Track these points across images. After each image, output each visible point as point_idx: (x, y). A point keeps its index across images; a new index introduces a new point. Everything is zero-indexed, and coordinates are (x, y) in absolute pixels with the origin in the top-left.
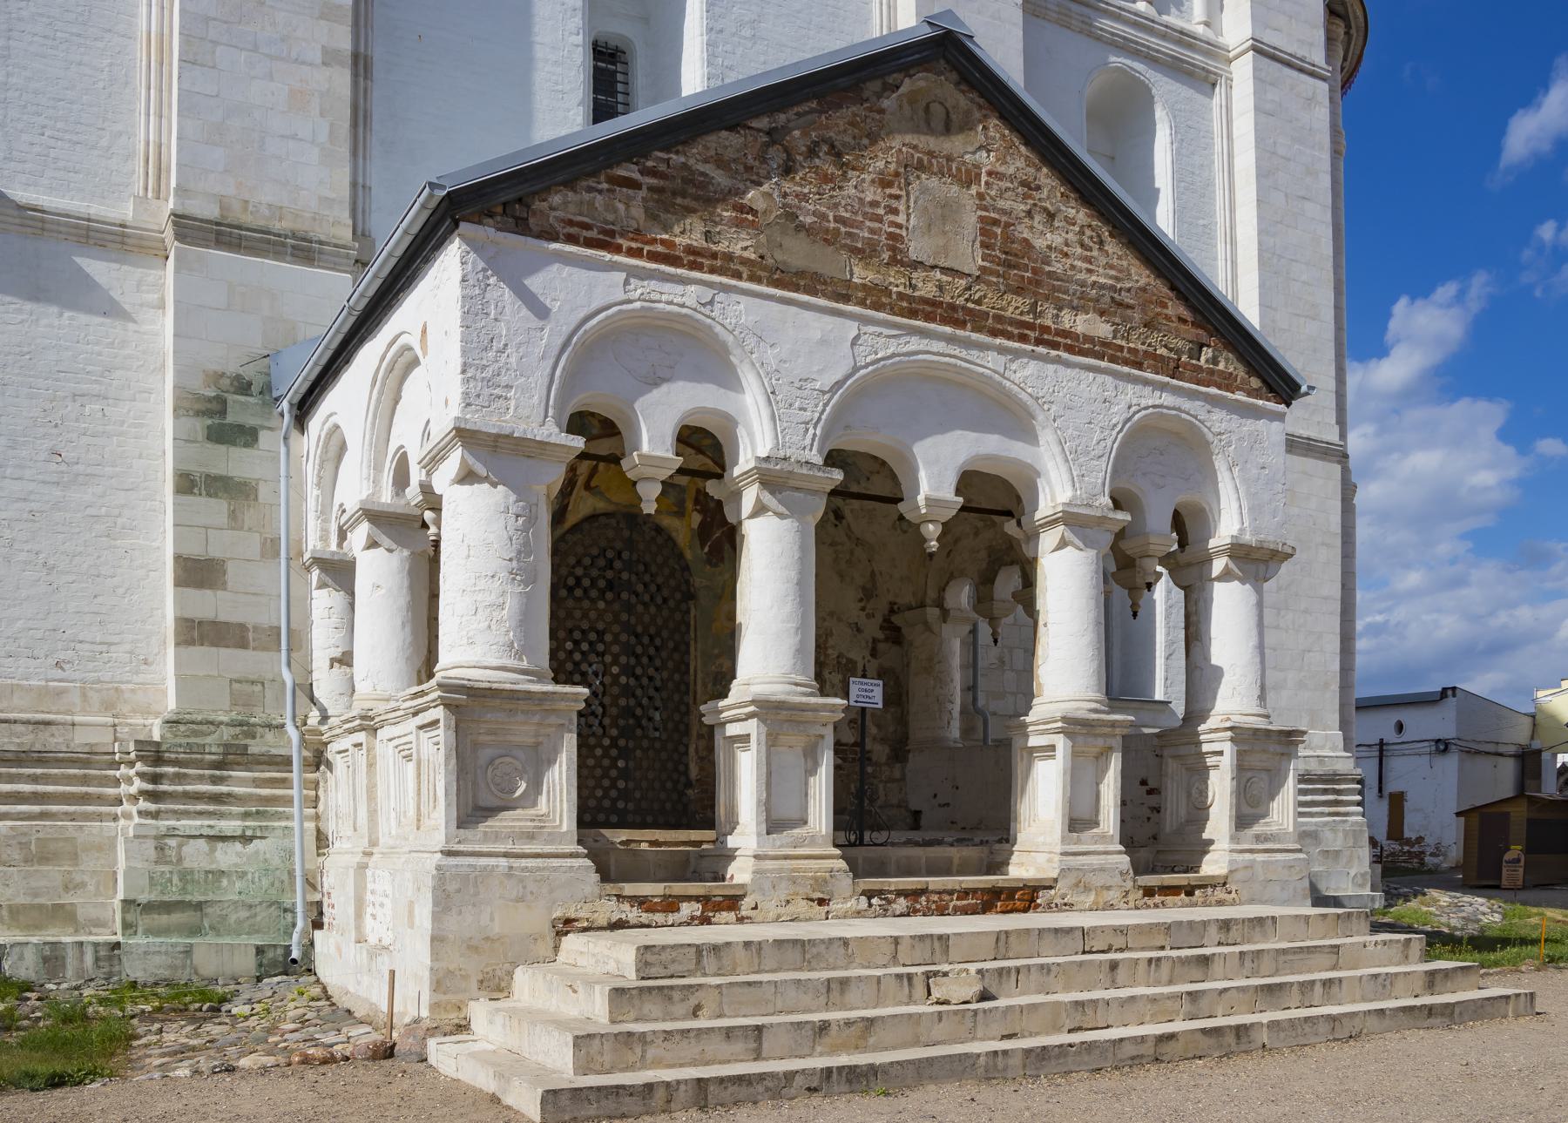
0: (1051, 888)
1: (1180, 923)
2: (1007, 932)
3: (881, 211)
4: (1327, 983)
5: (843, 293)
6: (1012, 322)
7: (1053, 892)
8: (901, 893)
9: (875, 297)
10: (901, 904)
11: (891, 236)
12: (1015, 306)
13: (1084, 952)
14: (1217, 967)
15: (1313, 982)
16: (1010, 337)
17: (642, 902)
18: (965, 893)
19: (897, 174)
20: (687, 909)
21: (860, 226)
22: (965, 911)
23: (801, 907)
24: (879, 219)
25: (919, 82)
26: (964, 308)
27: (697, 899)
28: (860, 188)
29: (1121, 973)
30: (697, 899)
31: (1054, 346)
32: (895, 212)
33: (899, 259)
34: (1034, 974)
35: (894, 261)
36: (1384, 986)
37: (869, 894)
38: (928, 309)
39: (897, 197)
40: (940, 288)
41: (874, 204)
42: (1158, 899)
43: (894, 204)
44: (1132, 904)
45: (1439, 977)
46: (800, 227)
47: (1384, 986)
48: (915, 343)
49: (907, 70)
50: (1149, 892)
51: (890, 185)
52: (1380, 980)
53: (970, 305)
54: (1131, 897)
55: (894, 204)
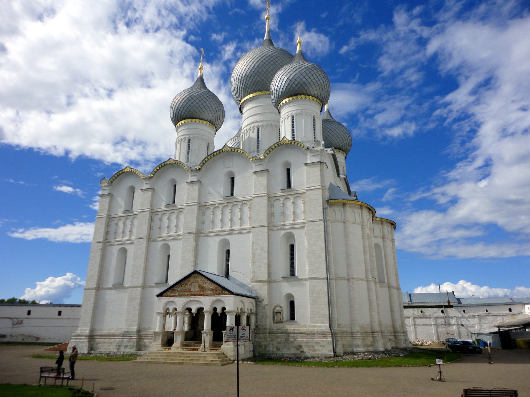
4: (198, 360)
5: (185, 296)
9: (187, 295)
10: (185, 349)
12: (202, 293)
17: (164, 349)
18: (191, 349)
20: (167, 349)
23: (176, 349)
25: (194, 275)
28: (188, 286)
33: (190, 291)
37: (182, 348)
46: (182, 291)
48: (191, 298)
49: (192, 274)
50: (211, 350)
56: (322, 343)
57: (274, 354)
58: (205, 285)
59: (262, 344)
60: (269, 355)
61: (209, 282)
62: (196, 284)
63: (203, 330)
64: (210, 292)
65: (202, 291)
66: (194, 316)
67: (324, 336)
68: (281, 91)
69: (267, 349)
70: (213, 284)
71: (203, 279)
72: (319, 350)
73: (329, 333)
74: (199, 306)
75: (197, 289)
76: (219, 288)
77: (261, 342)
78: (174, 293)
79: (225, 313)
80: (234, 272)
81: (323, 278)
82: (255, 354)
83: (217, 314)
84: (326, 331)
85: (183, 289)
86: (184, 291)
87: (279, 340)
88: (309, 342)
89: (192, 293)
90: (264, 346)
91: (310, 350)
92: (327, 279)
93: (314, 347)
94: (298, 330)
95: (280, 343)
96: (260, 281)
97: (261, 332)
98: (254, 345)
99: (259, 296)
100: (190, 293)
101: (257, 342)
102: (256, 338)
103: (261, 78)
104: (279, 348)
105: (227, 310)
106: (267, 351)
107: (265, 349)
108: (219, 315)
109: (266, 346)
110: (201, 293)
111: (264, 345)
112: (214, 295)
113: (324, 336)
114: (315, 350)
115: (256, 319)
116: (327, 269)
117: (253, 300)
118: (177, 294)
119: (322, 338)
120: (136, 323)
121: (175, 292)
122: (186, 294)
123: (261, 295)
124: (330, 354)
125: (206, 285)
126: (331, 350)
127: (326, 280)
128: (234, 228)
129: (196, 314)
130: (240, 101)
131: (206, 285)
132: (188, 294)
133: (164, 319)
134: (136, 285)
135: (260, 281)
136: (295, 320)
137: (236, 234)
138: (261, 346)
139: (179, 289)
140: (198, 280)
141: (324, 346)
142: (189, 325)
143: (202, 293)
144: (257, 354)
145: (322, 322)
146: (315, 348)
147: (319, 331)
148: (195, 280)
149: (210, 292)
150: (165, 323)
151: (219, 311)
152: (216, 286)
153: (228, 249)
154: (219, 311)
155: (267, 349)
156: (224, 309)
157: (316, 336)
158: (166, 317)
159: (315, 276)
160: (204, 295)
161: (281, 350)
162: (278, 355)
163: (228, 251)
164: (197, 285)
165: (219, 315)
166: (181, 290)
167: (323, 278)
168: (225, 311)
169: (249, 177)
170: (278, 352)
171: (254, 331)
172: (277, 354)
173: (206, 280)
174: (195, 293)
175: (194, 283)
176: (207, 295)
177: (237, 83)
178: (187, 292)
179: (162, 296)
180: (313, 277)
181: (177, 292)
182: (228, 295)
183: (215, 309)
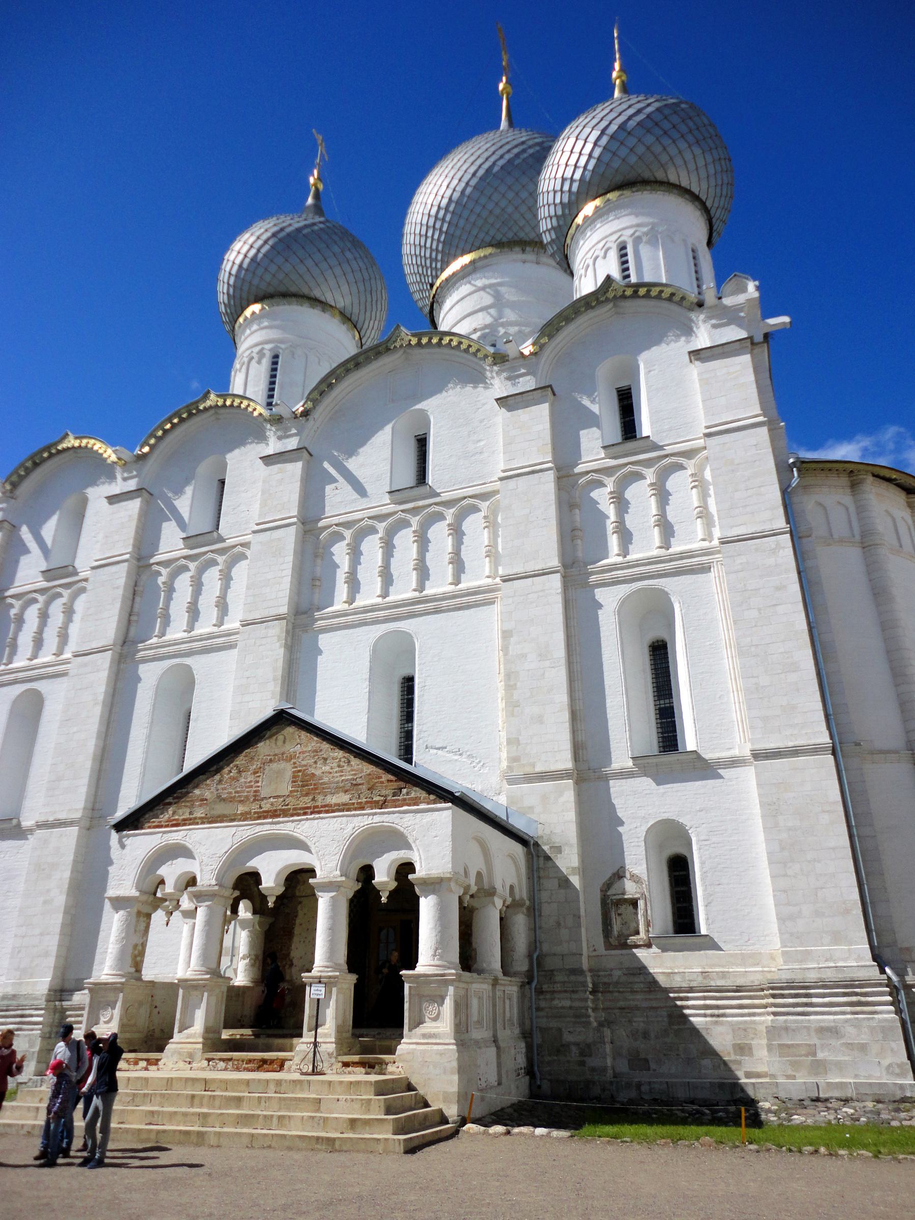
0: (291, 1060)
1: (254, 1080)
2: (172, 1078)
3: (253, 783)
4: (280, 1118)
6: (301, 809)
7: (291, 1062)
8: (220, 1060)
10: (222, 1065)
11: (255, 791)
13: (205, 1091)
14: (245, 1103)
15: (272, 1116)
16: (298, 815)
18: (250, 1061)
19: (260, 768)
20: (143, 1064)
21: (243, 792)
22: (249, 1070)
23: (181, 1064)
24: (251, 787)
26: (280, 810)
27: (146, 1060)
28: (247, 777)
29: (196, 1101)
30: (146, 1060)
31: (320, 812)
32: (258, 782)
33: (257, 798)
34: (158, 1098)
35: (255, 800)
36: (319, 1124)
37: (209, 1060)
38: (265, 814)
39: (259, 776)
40: (272, 804)
41: (251, 782)
42: (350, 1069)
43: (258, 779)
44: (334, 1071)
45: (359, 1123)
47: (319, 1124)
48: (258, 828)
50: (346, 1064)
51: (257, 772)
52: (316, 1120)
53: (284, 807)
54: (334, 1067)
55: (258, 779)
56: (850, 1030)
57: (629, 1085)
58: (320, 770)
59: (568, 1038)
60: (604, 1090)
61: (339, 754)
62: (283, 765)
63: (309, 970)
64: (344, 798)
65: (307, 795)
66: (270, 905)
67: (854, 999)
68: (577, 176)
69: (592, 1062)
70: (355, 762)
71: (314, 742)
72: (840, 1066)
73: (881, 985)
74: (294, 858)
75: (285, 788)
76: (386, 777)
77: (560, 1030)
78: (188, 810)
79: (411, 885)
80: (432, 751)
81: (815, 750)
82: (539, 1087)
83: (377, 893)
84: (862, 974)
85: (227, 790)
86: (231, 800)
87: (639, 1022)
88: (786, 1029)
89: (266, 806)
90: (574, 1049)
91: (795, 1065)
92: (834, 753)
93: (814, 1054)
94: (724, 975)
95: (646, 1035)
96: (543, 777)
97: (558, 987)
98: (529, 1048)
99: (540, 833)
100: (254, 808)
101: (542, 1030)
102: (541, 1014)
103: (497, 204)
104: (642, 1056)
105: (421, 871)
106: (593, 1070)
107: (582, 1063)
108: (384, 900)
109: (586, 1050)
110: (302, 805)
111: (577, 1044)
112: (363, 808)
113: (854, 999)
114: (819, 1067)
115: (534, 929)
116: (827, 716)
117: (518, 849)
118: (199, 813)
119: (848, 1009)
120: (51, 961)
121: (193, 806)
122: (241, 809)
123: (547, 831)
124: (902, 1087)
125: (327, 768)
126: (900, 1066)
127: (831, 758)
128: (429, 591)
129: (279, 898)
130: (432, 286)
131: (327, 768)
132: (246, 809)
133: (142, 926)
134: (62, 816)
135: (543, 777)
136: (703, 931)
137: (437, 611)
138: (561, 1049)
139: (207, 794)
140: (291, 748)
141: (863, 1048)
142: (253, 965)
143: (306, 801)
144: (546, 1086)
145: (837, 937)
146: (821, 1055)
147: (830, 975)
148: (277, 751)
149: (344, 798)
150: (144, 945)
151: (383, 877)
152: (368, 768)
153: (406, 672)
154: (383, 877)
155: (592, 1062)
156: (405, 869)
157: (815, 1000)
158: (149, 916)
159: (781, 745)
160: (315, 810)
161: (653, 1066)
162: (644, 1088)
163: (408, 684)
164: (288, 769)
165: (384, 900)
166: (219, 797)
167: (815, 750)
168: (410, 877)
169: (481, 421)
170: (640, 1076)
171: (529, 983)
172: (639, 1085)
173: (325, 746)
174: (279, 804)
175: (274, 766)
176: (329, 809)
177: (424, 229)
178: (241, 801)
179: (136, 828)
180: (772, 745)
181: (200, 806)
182: (423, 806)
183: (367, 872)
